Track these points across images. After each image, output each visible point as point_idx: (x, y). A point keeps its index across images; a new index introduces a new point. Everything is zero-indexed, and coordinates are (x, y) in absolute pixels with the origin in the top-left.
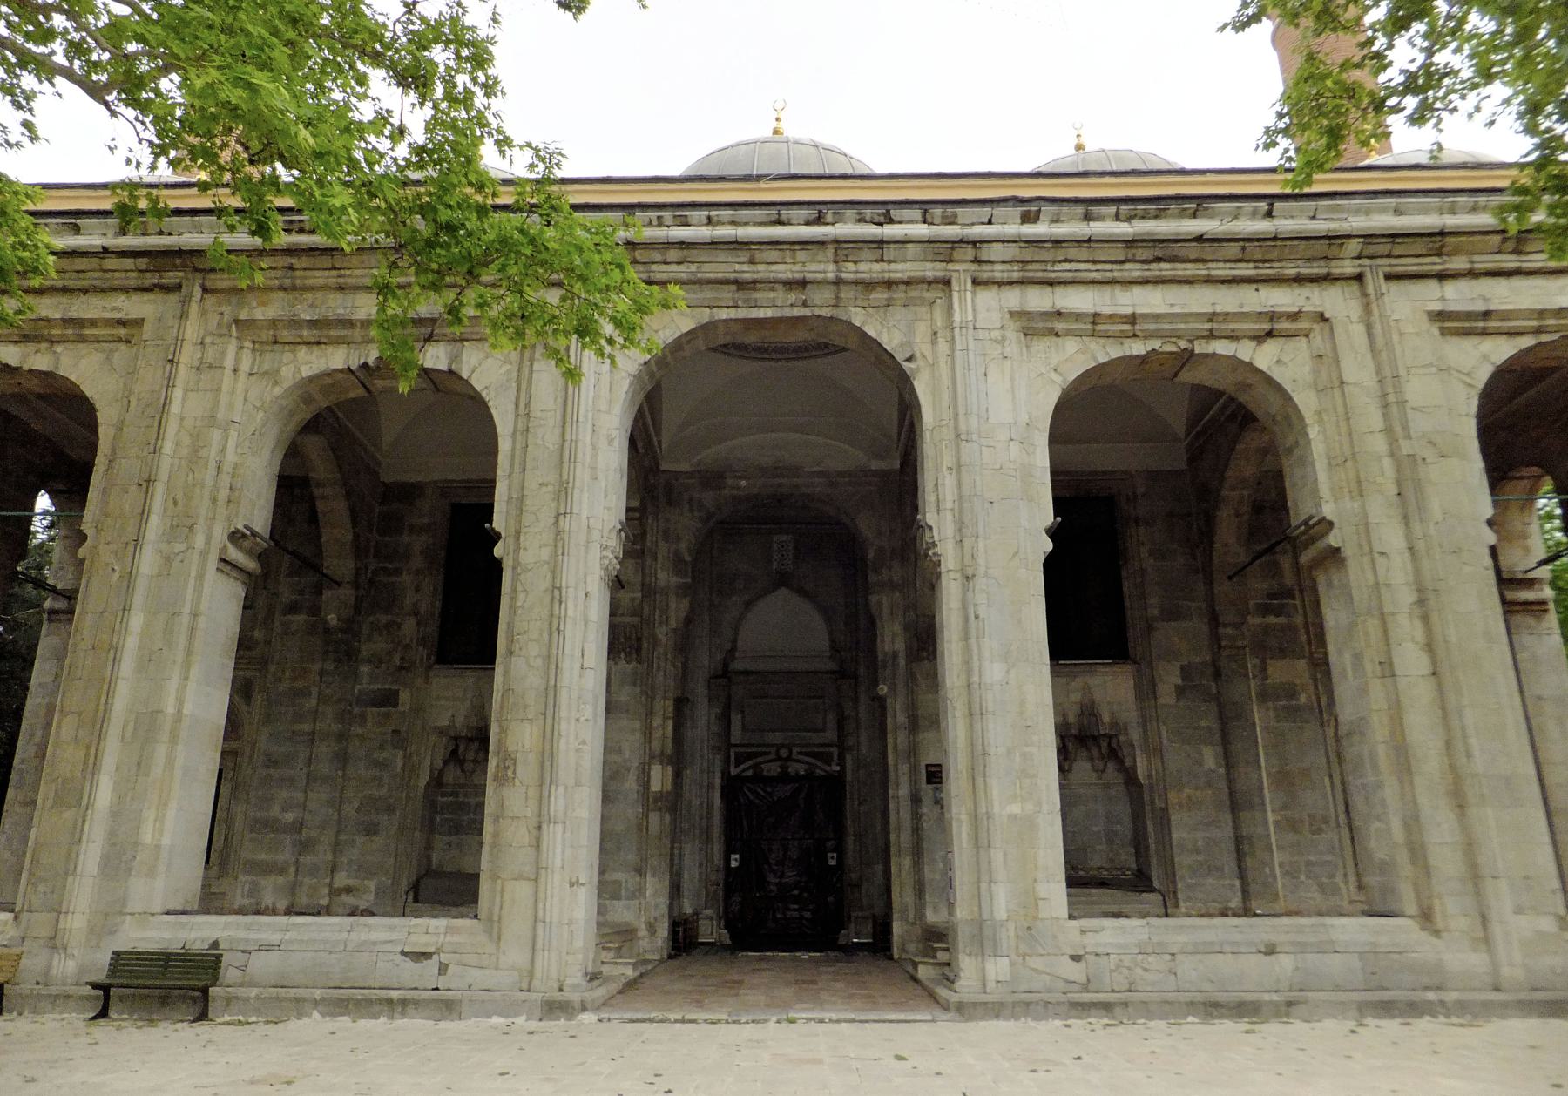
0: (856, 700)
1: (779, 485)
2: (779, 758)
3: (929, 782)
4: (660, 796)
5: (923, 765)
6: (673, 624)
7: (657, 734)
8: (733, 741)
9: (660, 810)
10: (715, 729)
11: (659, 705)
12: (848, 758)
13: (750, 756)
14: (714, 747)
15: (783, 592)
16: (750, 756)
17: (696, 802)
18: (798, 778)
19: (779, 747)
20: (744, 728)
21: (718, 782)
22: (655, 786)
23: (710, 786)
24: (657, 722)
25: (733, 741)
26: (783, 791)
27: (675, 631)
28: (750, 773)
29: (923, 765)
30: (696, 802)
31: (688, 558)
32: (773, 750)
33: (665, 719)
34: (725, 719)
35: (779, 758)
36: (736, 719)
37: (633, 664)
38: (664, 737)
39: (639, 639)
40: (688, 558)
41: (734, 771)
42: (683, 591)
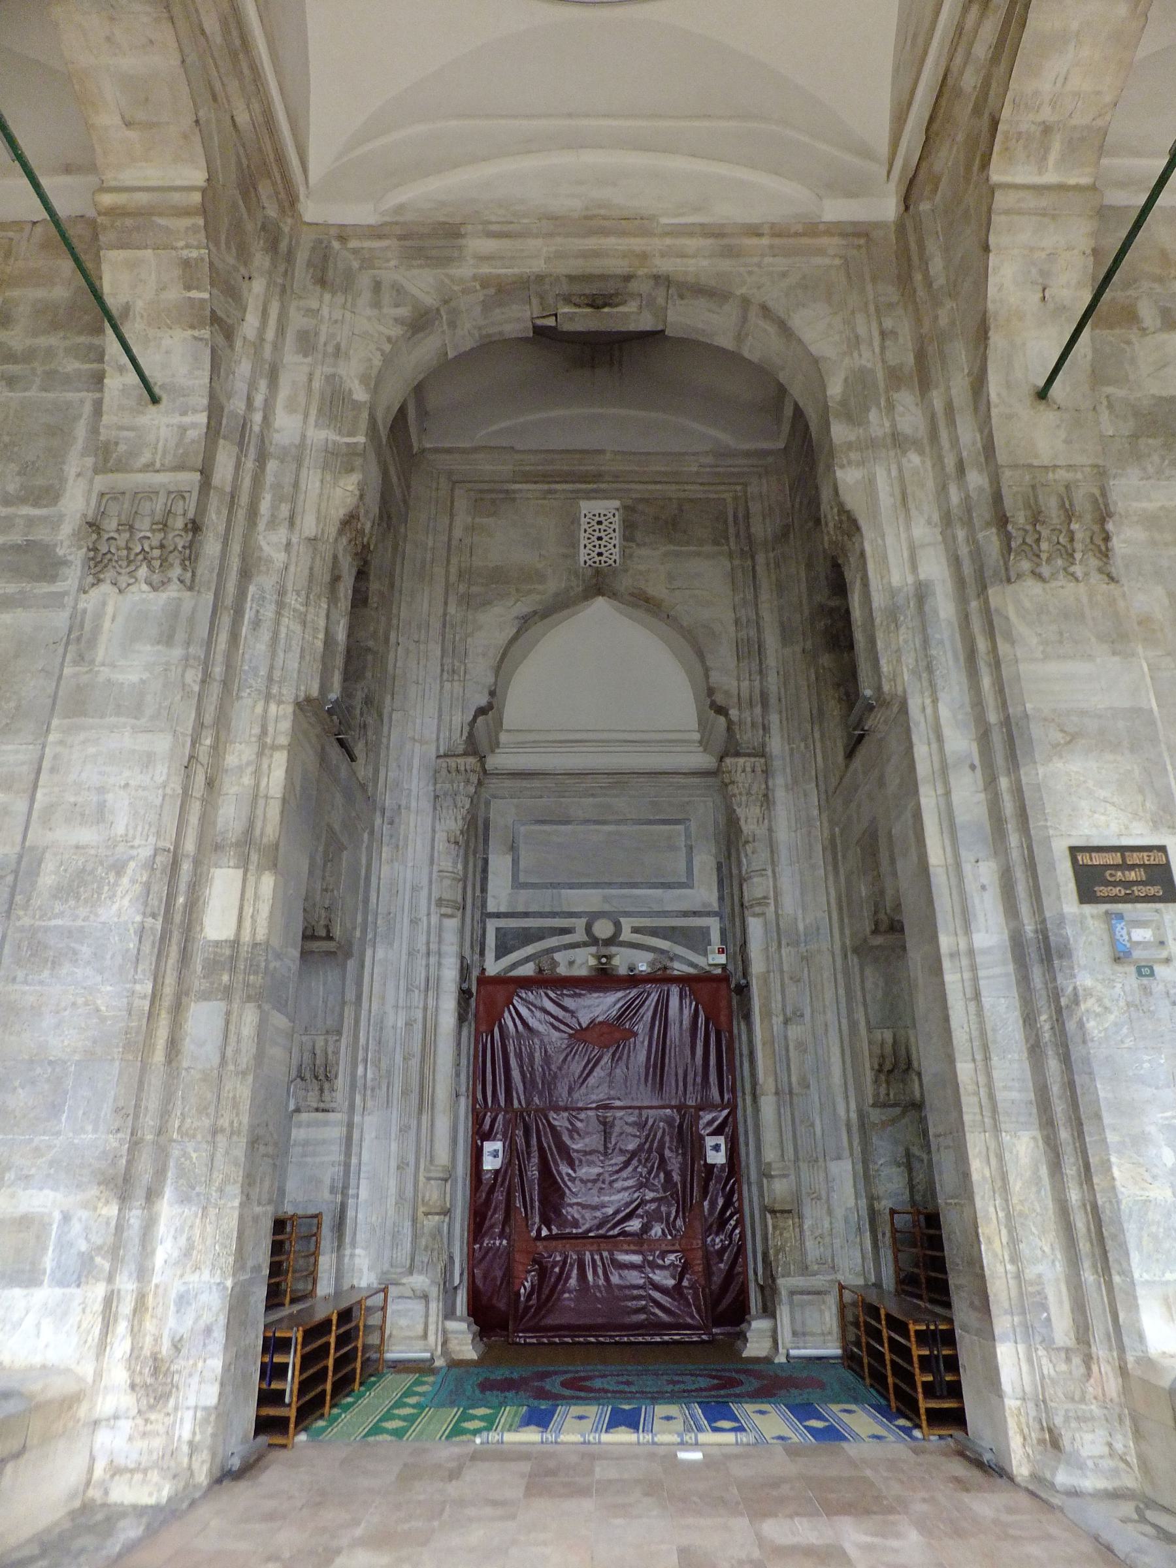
0: (767, 800)
1: (597, 254)
2: (594, 941)
3: (1086, 896)
4: (231, 955)
5: (1060, 848)
6: (309, 525)
7: (234, 789)
8: (491, 907)
9: (227, 993)
10: (446, 863)
11: (248, 712)
12: (755, 926)
13: (527, 937)
14: (440, 902)
15: (600, 604)
16: (527, 937)
17: (396, 1020)
18: (633, 980)
19: (593, 917)
20: (517, 884)
21: (450, 975)
22: (217, 925)
23: (431, 985)
24: (240, 754)
25: (491, 907)
26: (600, 1006)
27: (312, 540)
28: (528, 970)
29: (1060, 848)
30: (396, 1020)
31: (361, 395)
32: (580, 923)
33: (264, 749)
34: (475, 838)
35: (594, 941)
36: (500, 865)
37: (173, 592)
38: (255, 796)
39: (195, 527)
40: (361, 395)
41: (493, 968)
42: (339, 460)
